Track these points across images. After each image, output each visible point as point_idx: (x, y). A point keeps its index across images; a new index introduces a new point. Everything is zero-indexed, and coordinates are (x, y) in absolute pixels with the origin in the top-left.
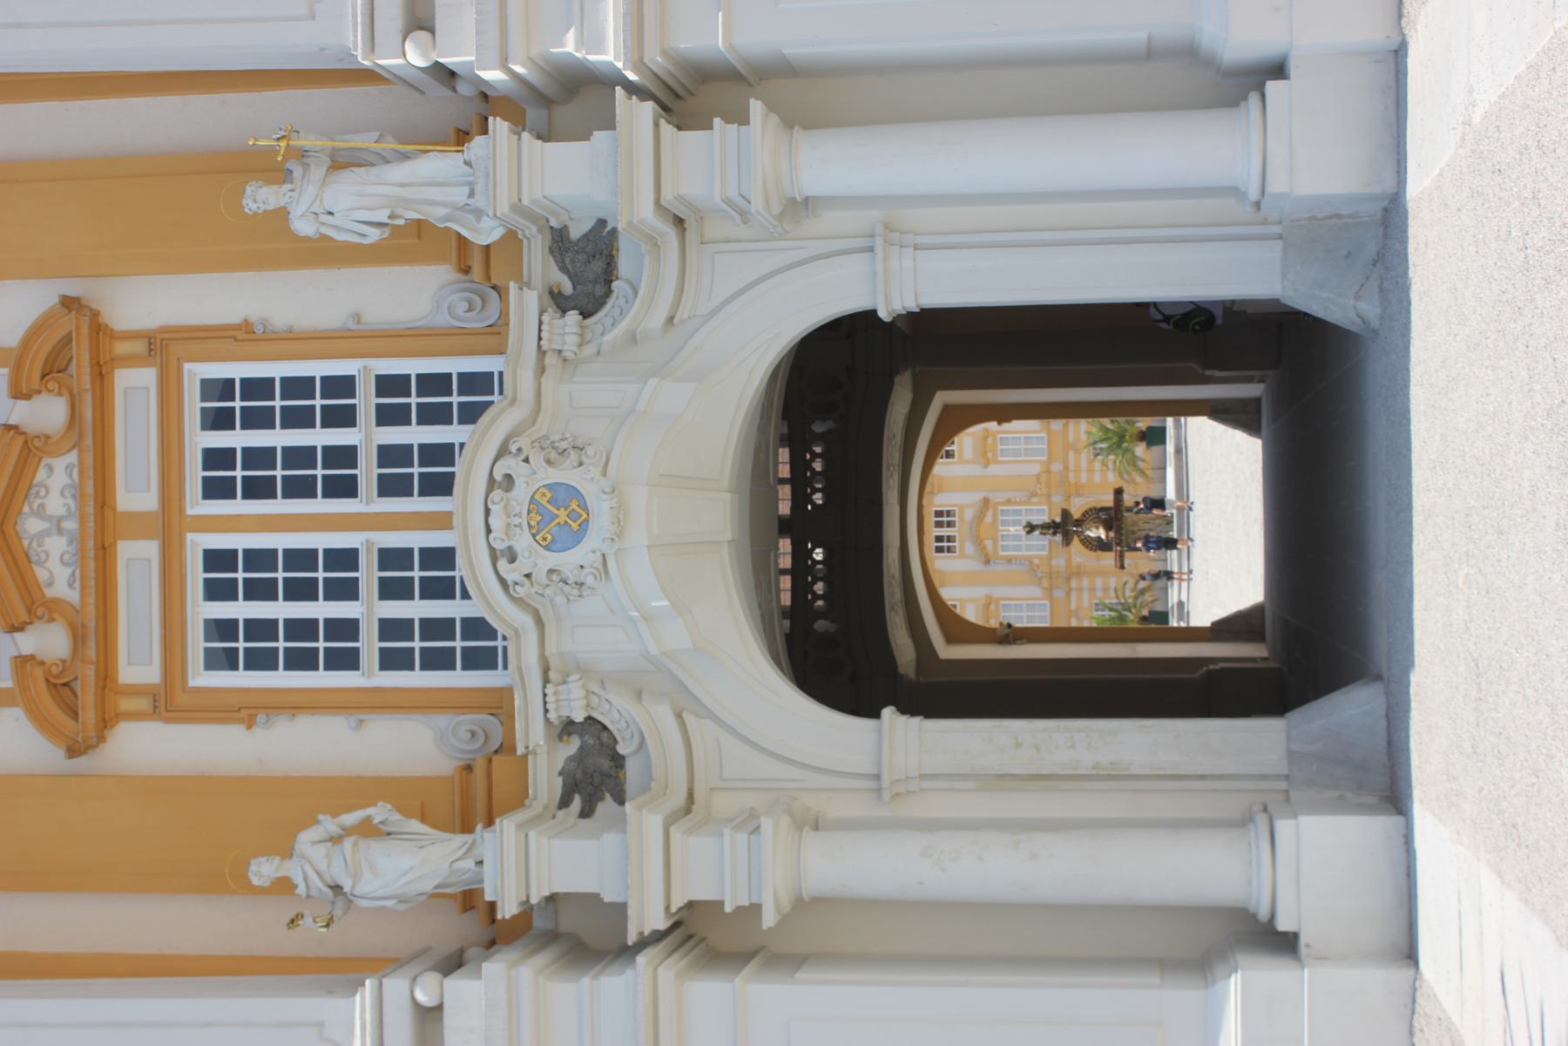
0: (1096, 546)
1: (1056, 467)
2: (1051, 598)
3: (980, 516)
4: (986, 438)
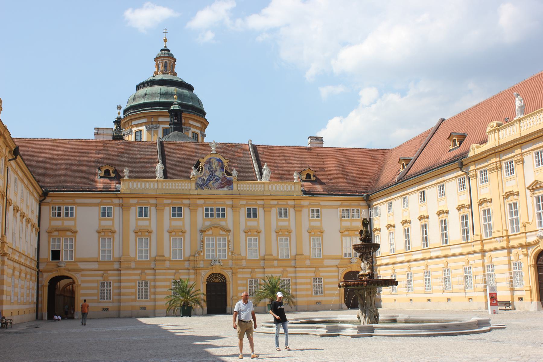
0: (209, 281)
1: (244, 263)
2: (184, 261)
3: (223, 229)
4: (257, 232)
